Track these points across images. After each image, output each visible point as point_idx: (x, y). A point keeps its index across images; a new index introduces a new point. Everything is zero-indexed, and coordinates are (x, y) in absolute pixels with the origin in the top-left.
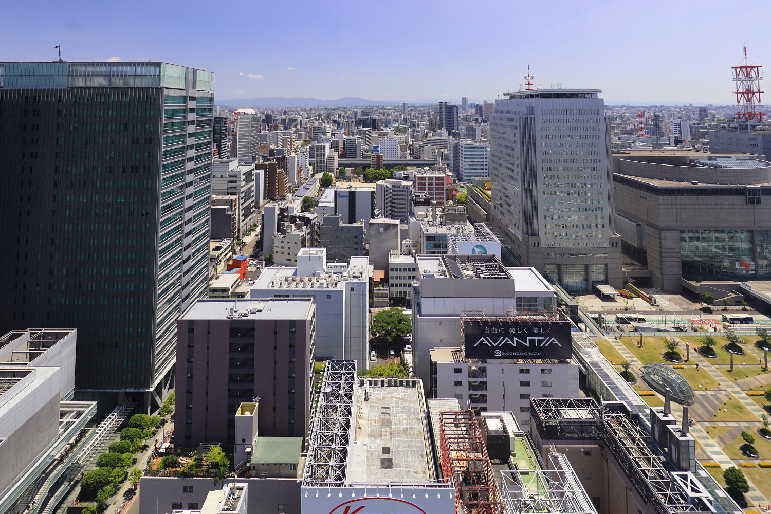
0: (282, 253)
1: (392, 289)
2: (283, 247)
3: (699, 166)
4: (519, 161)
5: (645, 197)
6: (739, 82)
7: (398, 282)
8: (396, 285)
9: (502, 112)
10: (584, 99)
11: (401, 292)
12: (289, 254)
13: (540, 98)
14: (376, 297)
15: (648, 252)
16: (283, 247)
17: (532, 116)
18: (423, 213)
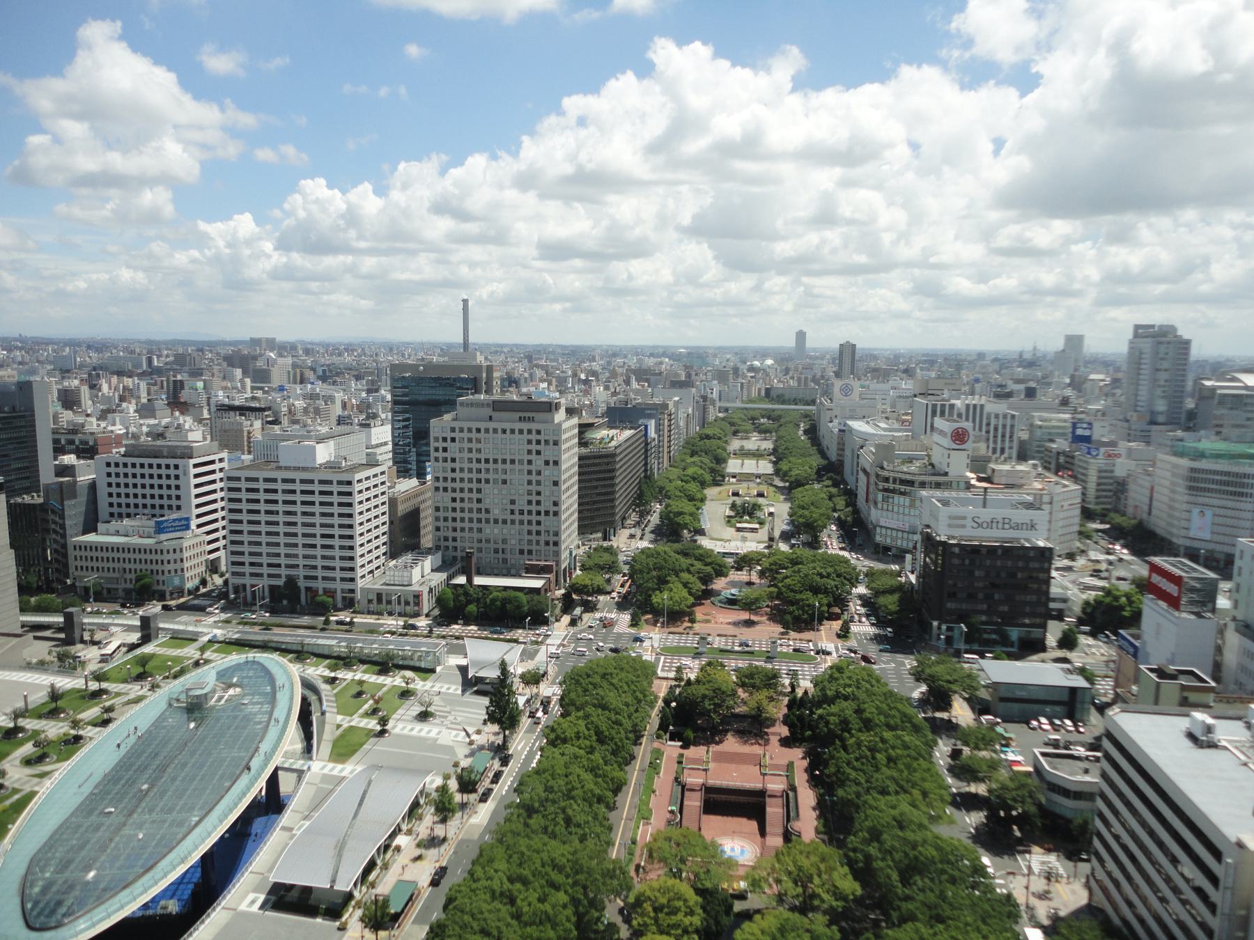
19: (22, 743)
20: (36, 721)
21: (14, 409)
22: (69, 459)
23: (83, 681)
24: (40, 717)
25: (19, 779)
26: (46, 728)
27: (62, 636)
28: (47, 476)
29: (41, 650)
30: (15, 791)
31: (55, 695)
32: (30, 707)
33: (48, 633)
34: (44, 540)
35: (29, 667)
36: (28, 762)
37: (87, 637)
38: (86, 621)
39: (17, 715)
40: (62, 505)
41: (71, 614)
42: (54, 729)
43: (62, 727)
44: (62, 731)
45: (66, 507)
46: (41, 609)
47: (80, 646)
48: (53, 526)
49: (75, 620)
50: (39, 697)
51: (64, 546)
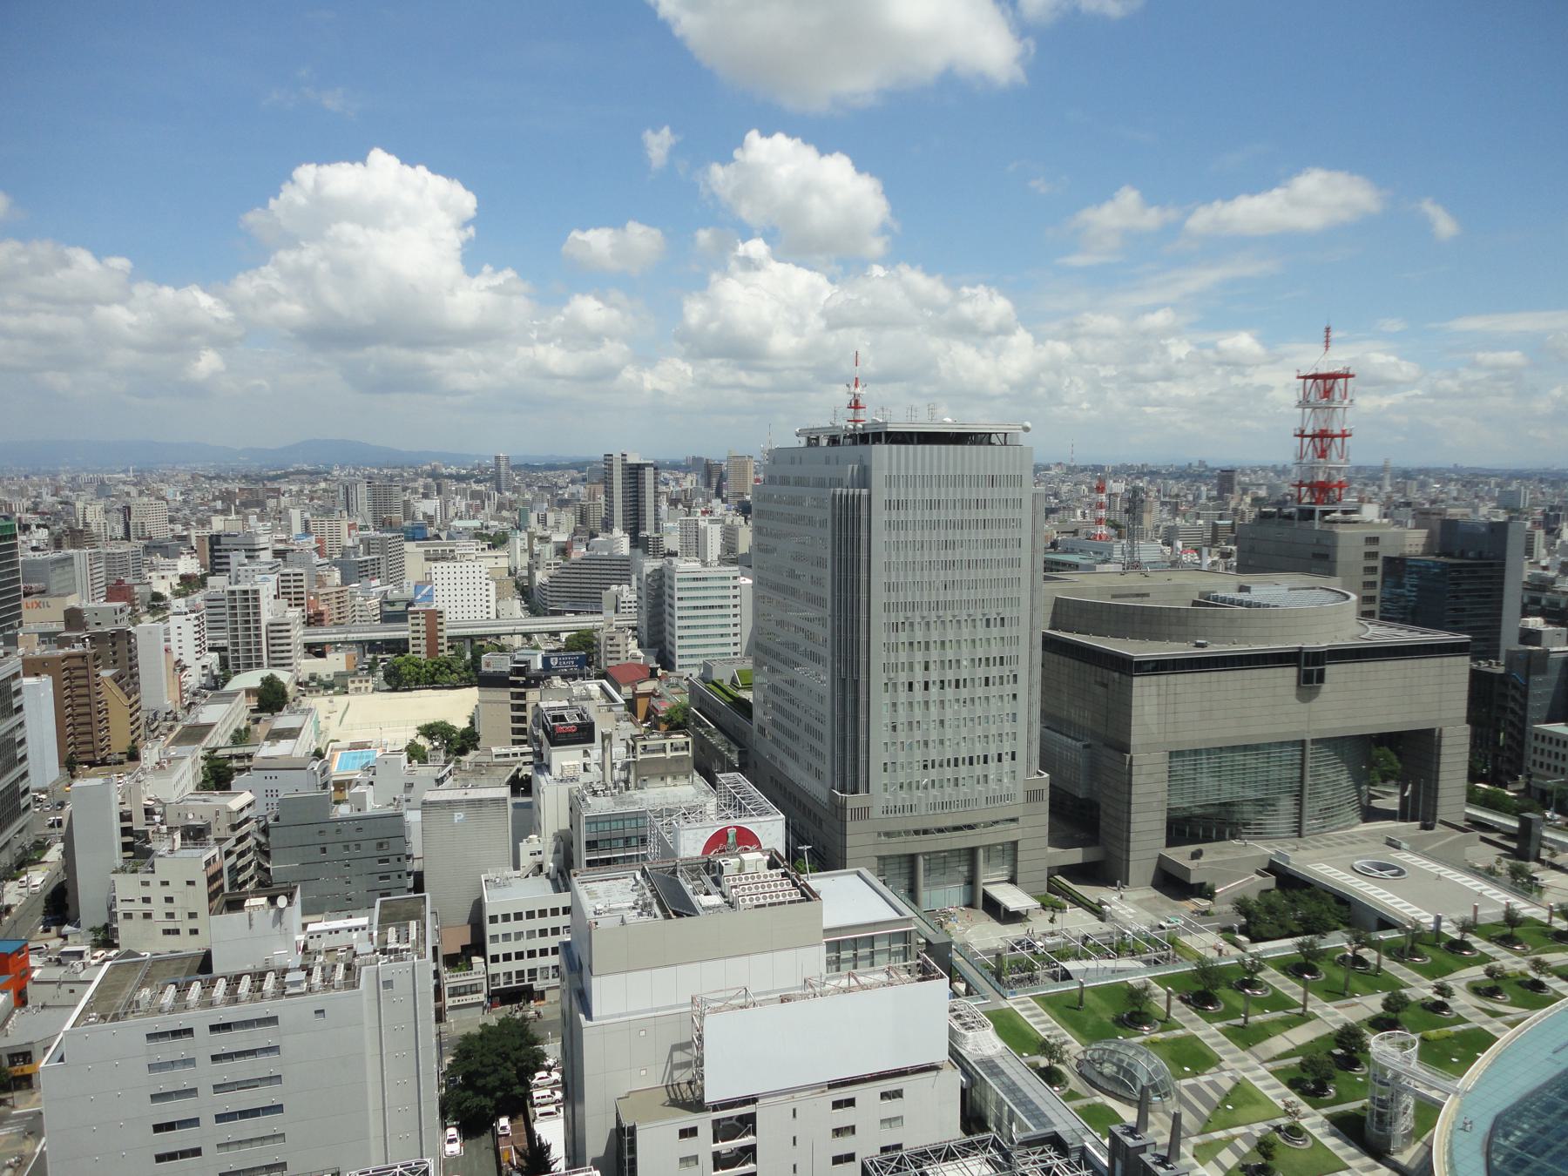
0: (147, 916)
1: (494, 968)
2: (146, 900)
3: (1216, 606)
4: (829, 612)
5: (1105, 681)
6: (1308, 411)
7: (512, 947)
8: (507, 957)
9: (785, 481)
10: (989, 447)
11: (520, 974)
12: (170, 915)
13: (886, 443)
14: (450, 996)
15: (1103, 806)
16: (146, 900)
17: (864, 492)
18: (576, 762)
19: (1469, 963)
20: (1486, 943)
21: (1480, 555)
22: (1535, 623)
23: (1546, 913)
24: (1490, 940)
25: (1465, 1007)
26: (1498, 956)
27: (1514, 845)
28: (1509, 641)
29: (1486, 855)
30: (1461, 1020)
31: (1511, 919)
32: (1480, 922)
33: (1494, 837)
34: (1498, 719)
35: (1474, 871)
36: (1476, 990)
37: (1545, 855)
38: (1547, 834)
39: (1466, 927)
40: (1527, 680)
41: (1530, 820)
42: (1511, 962)
43: (1517, 963)
44: (1519, 967)
45: (1531, 683)
46: (1489, 803)
47: (1533, 865)
48: (1512, 705)
49: (1534, 829)
50: (1491, 914)
51: (1522, 731)
